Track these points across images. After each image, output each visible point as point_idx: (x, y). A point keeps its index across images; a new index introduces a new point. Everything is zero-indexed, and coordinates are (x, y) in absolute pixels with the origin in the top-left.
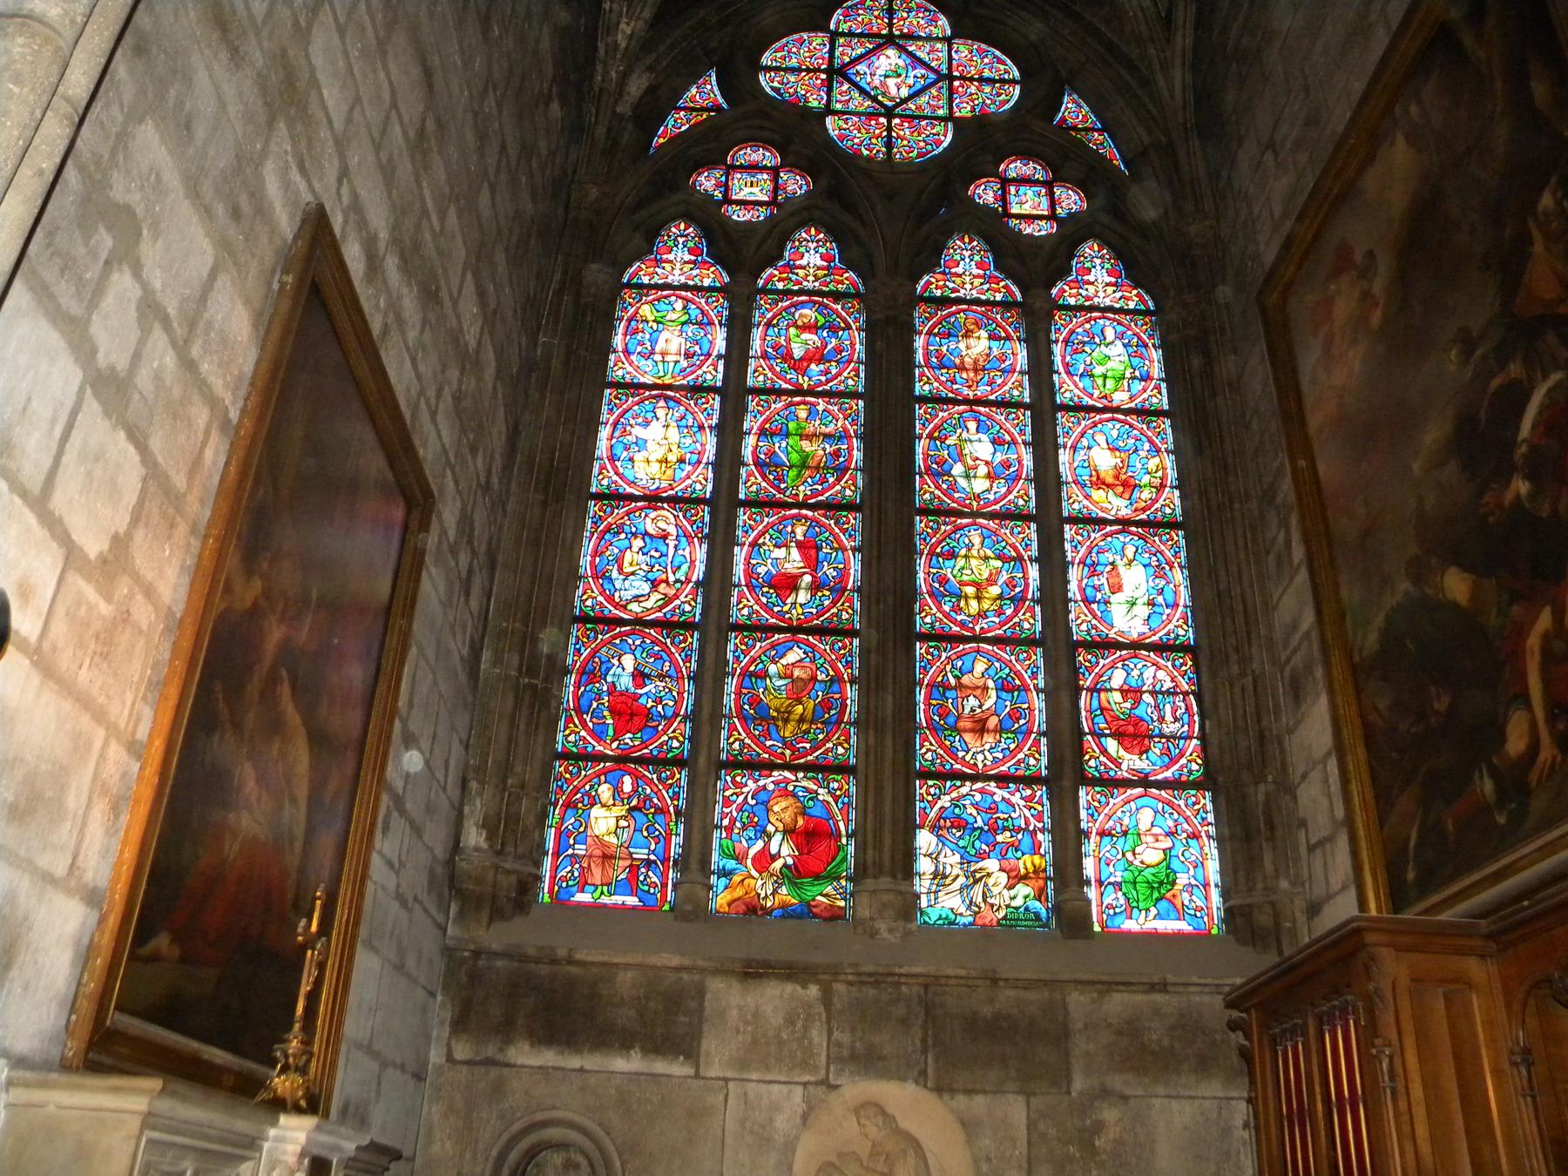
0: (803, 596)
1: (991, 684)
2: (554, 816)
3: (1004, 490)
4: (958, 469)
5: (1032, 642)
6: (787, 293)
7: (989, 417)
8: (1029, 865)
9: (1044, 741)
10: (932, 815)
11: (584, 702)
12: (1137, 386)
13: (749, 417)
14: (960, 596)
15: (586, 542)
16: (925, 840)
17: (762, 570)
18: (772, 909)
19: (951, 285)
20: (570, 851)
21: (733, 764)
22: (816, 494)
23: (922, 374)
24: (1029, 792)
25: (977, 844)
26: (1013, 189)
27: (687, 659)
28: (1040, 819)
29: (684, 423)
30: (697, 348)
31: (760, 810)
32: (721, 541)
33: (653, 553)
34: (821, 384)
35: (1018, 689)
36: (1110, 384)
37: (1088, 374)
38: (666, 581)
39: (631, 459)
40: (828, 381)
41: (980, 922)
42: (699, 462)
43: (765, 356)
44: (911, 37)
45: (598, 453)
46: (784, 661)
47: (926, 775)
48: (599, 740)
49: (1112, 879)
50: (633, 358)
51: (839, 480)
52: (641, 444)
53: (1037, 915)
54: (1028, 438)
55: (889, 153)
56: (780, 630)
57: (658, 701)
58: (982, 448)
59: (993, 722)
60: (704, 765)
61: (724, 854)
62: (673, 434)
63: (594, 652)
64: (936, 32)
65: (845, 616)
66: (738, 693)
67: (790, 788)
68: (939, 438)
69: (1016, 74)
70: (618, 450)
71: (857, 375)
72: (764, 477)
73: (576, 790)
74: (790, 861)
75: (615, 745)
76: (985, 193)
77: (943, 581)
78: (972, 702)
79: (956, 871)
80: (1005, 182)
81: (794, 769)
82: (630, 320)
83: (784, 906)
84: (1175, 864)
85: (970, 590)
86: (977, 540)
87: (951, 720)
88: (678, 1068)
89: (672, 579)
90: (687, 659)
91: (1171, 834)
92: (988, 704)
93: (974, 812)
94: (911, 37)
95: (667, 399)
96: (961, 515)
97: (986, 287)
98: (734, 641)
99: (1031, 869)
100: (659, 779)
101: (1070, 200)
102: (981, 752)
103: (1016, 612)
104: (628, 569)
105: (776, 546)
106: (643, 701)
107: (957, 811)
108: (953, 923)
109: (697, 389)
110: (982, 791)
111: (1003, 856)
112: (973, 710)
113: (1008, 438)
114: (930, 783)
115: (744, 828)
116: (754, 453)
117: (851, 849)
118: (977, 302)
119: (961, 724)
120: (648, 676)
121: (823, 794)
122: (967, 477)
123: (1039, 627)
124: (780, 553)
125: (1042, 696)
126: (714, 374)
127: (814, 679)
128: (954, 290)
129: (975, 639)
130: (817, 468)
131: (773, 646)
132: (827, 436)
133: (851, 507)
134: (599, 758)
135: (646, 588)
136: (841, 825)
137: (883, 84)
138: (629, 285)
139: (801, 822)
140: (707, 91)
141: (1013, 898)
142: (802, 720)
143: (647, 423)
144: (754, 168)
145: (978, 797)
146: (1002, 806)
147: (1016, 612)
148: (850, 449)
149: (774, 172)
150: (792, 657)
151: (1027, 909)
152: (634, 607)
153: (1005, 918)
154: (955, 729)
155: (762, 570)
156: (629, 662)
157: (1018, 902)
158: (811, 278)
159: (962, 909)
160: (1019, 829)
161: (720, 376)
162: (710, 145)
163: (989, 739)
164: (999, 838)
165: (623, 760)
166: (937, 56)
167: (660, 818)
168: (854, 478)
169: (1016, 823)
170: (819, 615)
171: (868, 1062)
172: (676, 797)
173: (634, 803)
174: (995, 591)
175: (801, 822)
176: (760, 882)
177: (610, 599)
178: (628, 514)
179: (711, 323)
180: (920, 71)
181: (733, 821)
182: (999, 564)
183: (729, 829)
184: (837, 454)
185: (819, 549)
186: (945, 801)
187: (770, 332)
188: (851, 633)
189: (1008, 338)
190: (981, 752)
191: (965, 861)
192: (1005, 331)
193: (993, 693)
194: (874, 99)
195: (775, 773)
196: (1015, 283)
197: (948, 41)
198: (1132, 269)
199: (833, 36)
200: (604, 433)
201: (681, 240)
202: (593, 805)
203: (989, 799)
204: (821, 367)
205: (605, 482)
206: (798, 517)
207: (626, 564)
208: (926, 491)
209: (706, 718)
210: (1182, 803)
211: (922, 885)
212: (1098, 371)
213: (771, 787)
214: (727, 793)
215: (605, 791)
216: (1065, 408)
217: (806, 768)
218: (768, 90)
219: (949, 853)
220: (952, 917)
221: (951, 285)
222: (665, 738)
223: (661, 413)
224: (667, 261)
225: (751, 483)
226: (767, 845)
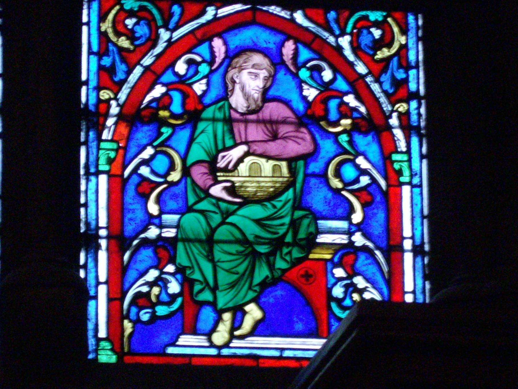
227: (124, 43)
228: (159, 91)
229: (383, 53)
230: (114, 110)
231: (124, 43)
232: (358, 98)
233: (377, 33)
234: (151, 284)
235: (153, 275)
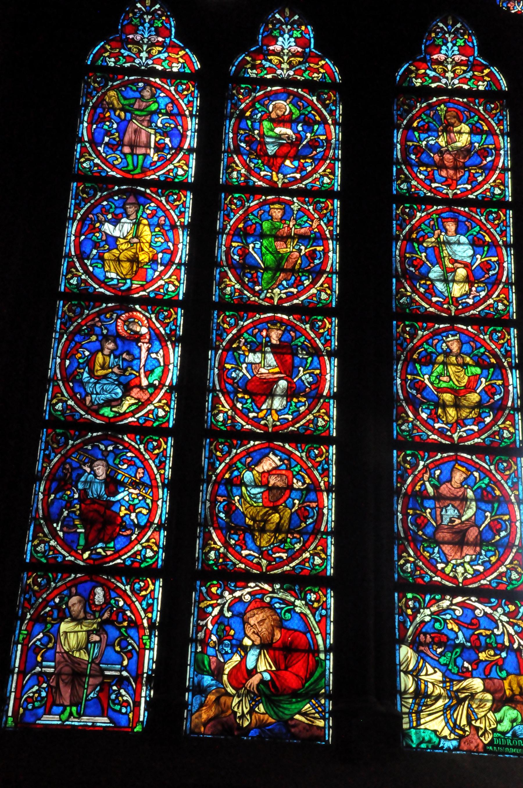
0: (278, 403)
1: (470, 494)
2: (21, 631)
3: (483, 294)
4: (436, 272)
6: (263, 83)
7: (470, 218)
8: (515, 686)
11: (54, 510)
13: (220, 215)
15: (54, 344)
19: (432, 74)
20: (38, 669)
21: (208, 575)
22: (291, 297)
23: (400, 171)
24: (512, 608)
25: (459, 661)
27: (161, 466)
29: (156, 219)
30: (167, 140)
31: (236, 623)
34: (295, 181)
38: (140, 386)
39: (101, 258)
40: (303, 179)
41: (465, 747)
42: (171, 262)
43: (237, 150)
45: (66, 250)
46: (260, 469)
47: (404, 586)
48: (71, 550)
50: (101, 149)
51: (313, 283)
52: (112, 242)
56: (254, 436)
58: (463, 251)
59: (472, 534)
61: (200, 669)
63: (66, 457)
65: (321, 422)
68: (417, 240)
70: (87, 248)
71: (333, 173)
73: (46, 602)
74: (267, 677)
75: (86, 555)
77: (421, 387)
78: (451, 512)
81: (271, 580)
82: (94, 108)
83: (261, 725)
85: (448, 397)
86: (455, 347)
87: (429, 530)
89: (145, 382)
90: (161, 466)
92: (469, 513)
93: (456, 629)
96: (440, 320)
97: (469, 75)
99: (517, 691)
100: (132, 590)
103: (494, 422)
105: (251, 351)
106: (115, 508)
107: (437, 625)
108: (436, 747)
112: (451, 521)
113: (487, 239)
114: (410, 595)
115: (220, 641)
116: (227, 253)
117: (330, 664)
118: (459, 92)
119: (440, 535)
120: (122, 484)
122: (445, 281)
127: (290, 487)
128: (435, 79)
130: (292, 271)
131: (248, 453)
132: (302, 238)
133: (327, 311)
134: (70, 568)
136: (319, 638)
138: (94, 68)
139: (278, 635)
141: (500, 722)
142: (278, 529)
143: (116, 221)
145: (459, 612)
146: (484, 622)
147: (494, 422)
148: (326, 252)
150: (266, 465)
151: (514, 735)
152: (106, 411)
153: (491, 743)
156: (101, 471)
157: (505, 726)
158: (285, 66)
159: (446, 732)
160: (502, 647)
161: (192, 172)
164: (482, 656)
167: (132, 632)
168: (329, 281)
169: (500, 641)
170: (295, 420)
172: (149, 608)
173: (106, 616)
174: (474, 398)
175: (278, 635)
176: (236, 700)
177: (81, 403)
178: (98, 314)
179: (181, 114)
181: (209, 633)
182: (478, 370)
183: (204, 643)
184: (312, 255)
185: (295, 354)
186: (425, 615)
187: (243, 125)
188: (328, 441)
189: (491, 132)
190: (462, 565)
191: (448, 679)
192: (488, 124)
193: (474, 503)
195: (252, 584)
196: (501, 71)
200: (72, 229)
201: (147, 18)
202: (61, 619)
203: (469, 612)
204: (296, 163)
205: (74, 281)
206: (274, 321)
207: (97, 367)
213: (248, 598)
214: (202, 605)
219: (431, 670)
220: (435, 740)
221: (432, 74)
222: (138, 547)
223: (131, 210)
224: (134, 42)
226: (244, 659)
227: (36, 588)
228: (48, 609)
229: (143, 593)
230: (29, 616)
231: (36, 588)
232: (132, 612)
233: (142, 584)
234: (34, 693)
235: (36, 688)
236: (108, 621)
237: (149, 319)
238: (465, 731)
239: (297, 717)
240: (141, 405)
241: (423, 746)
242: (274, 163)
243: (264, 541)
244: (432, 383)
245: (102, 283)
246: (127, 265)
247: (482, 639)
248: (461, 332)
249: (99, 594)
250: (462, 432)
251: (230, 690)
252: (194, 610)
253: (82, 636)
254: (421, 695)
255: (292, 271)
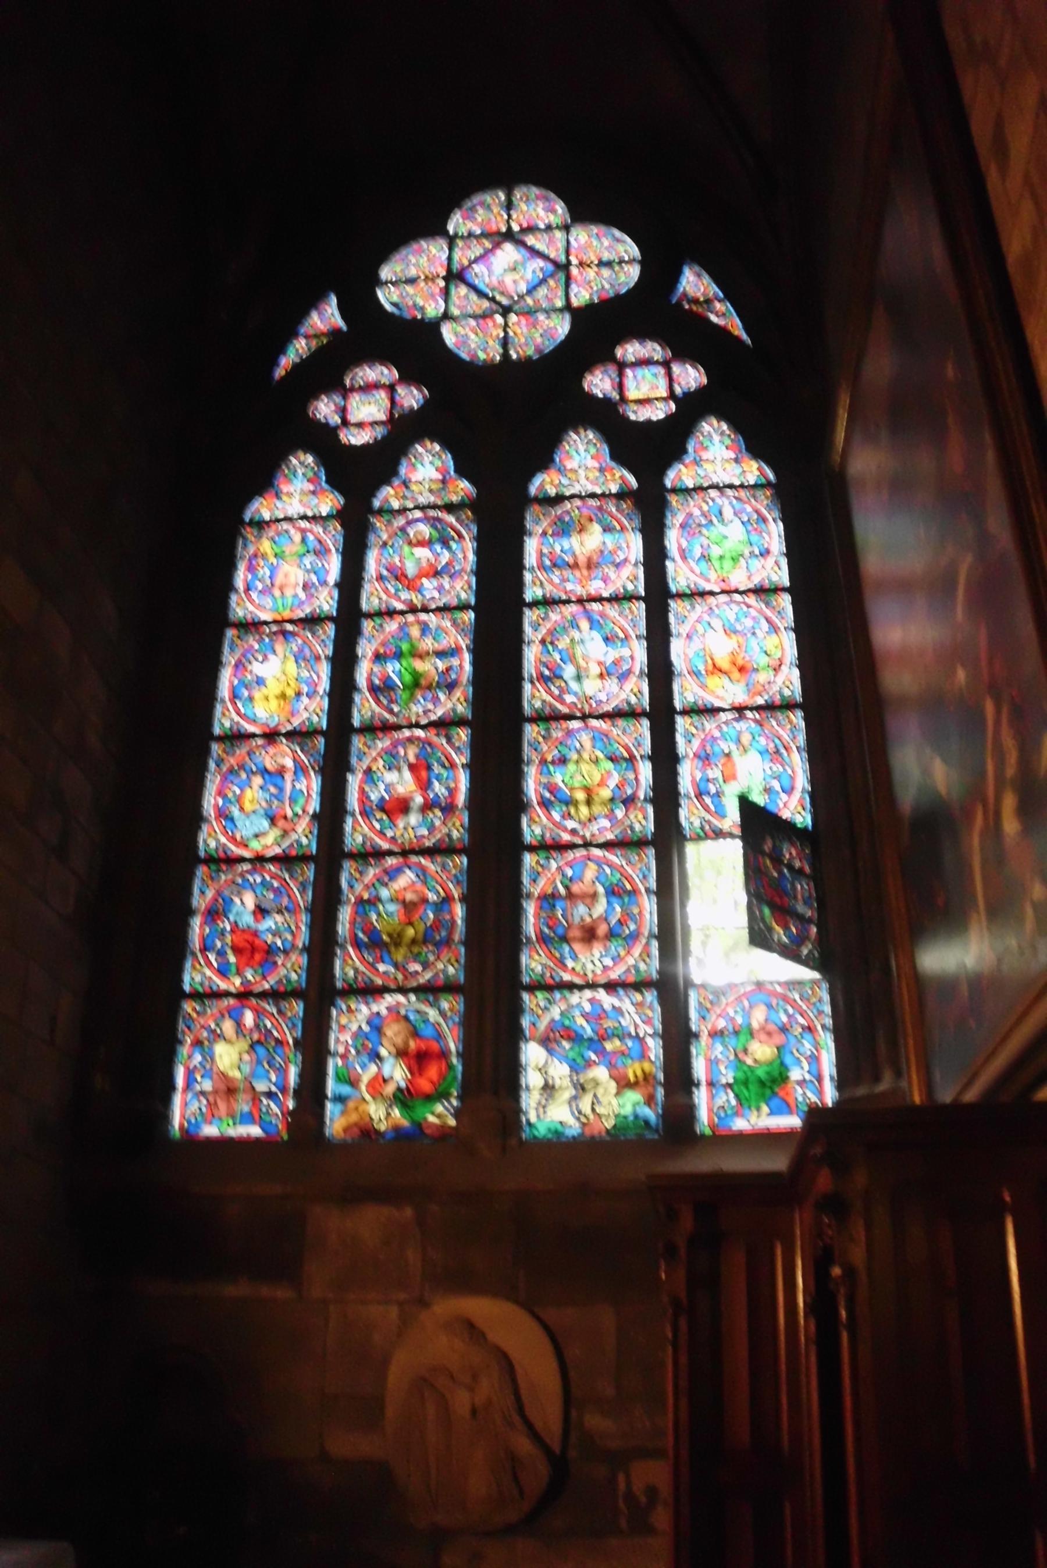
0: (414, 819)
1: (601, 890)
4: (569, 672)
5: (640, 844)
6: (403, 511)
7: (602, 615)
9: (655, 944)
10: (542, 1025)
12: (756, 564)
14: (570, 802)
16: (532, 1053)
17: (374, 797)
18: (385, 1132)
20: (198, 1088)
26: (629, 372)
28: (648, 1022)
31: (374, 1037)
32: (334, 769)
33: (273, 790)
35: (629, 893)
36: (728, 564)
37: (705, 557)
38: (285, 817)
39: (251, 699)
43: (380, 578)
44: (531, 229)
47: (532, 988)
49: (724, 1081)
52: (260, 682)
53: (647, 1123)
54: (642, 630)
55: (506, 355)
57: (276, 933)
60: (320, 995)
61: (339, 1079)
62: (291, 667)
64: (554, 220)
66: (353, 922)
67: (403, 1012)
69: (634, 251)
72: (378, 702)
74: (403, 1084)
76: (599, 383)
77: (553, 789)
79: (567, 1082)
80: (622, 366)
83: (397, 1129)
84: (788, 1060)
85: (580, 796)
86: (588, 744)
88: (282, 1293)
91: (784, 1029)
94: (531, 229)
95: (284, 633)
98: (348, 871)
101: (691, 377)
102: (592, 961)
104: (248, 806)
109: (312, 621)
110: (592, 1001)
111: (611, 1066)
118: (593, 495)
121: (433, 1014)
123: (651, 827)
124: (391, 777)
125: (654, 899)
126: (327, 602)
129: (587, 845)
132: (440, 654)
133: (461, 722)
135: (265, 824)
137: (501, 283)
139: (412, 1044)
140: (327, 316)
144: (370, 387)
145: (588, 1007)
146: (612, 1014)
149: (391, 389)
152: (256, 845)
154: (565, 939)
155: (374, 797)
156: (250, 900)
157: (627, 1110)
159: (571, 1121)
162: (328, 370)
163: (597, 949)
164: (609, 1046)
165: (244, 995)
166: (553, 246)
171: (462, 1280)
174: (606, 793)
177: (233, 839)
180: (541, 263)
182: (609, 765)
185: (429, 768)
186: (555, 1012)
194: (493, 300)
196: (631, 470)
197: (566, 228)
198: (755, 442)
199: (452, 241)
208: (534, 697)
209: (322, 946)
210: (797, 997)
211: (530, 1102)
212: (715, 552)
215: (228, 1027)
216: (681, 596)
217: (417, 990)
218: (388, 307)
225: (365, 708)
236: (259, 1042)
237: (294, 752)
238: (588, 1119)
239: (431, 1119)
240: (285, 833)
241: (550, 1136)
242: (412, 585)
243: (399, 955)
244: (566, 785)
245: (254, 721)
246: (274, 704)
247: (609, 1031)
248: (593, 729)
249: (249, 1018)
250: (594, 828)
251: (368, 1097)
252: (334, 1026)
253: (235, 1057)
254: (549, 1089)
255: (429, 687)
